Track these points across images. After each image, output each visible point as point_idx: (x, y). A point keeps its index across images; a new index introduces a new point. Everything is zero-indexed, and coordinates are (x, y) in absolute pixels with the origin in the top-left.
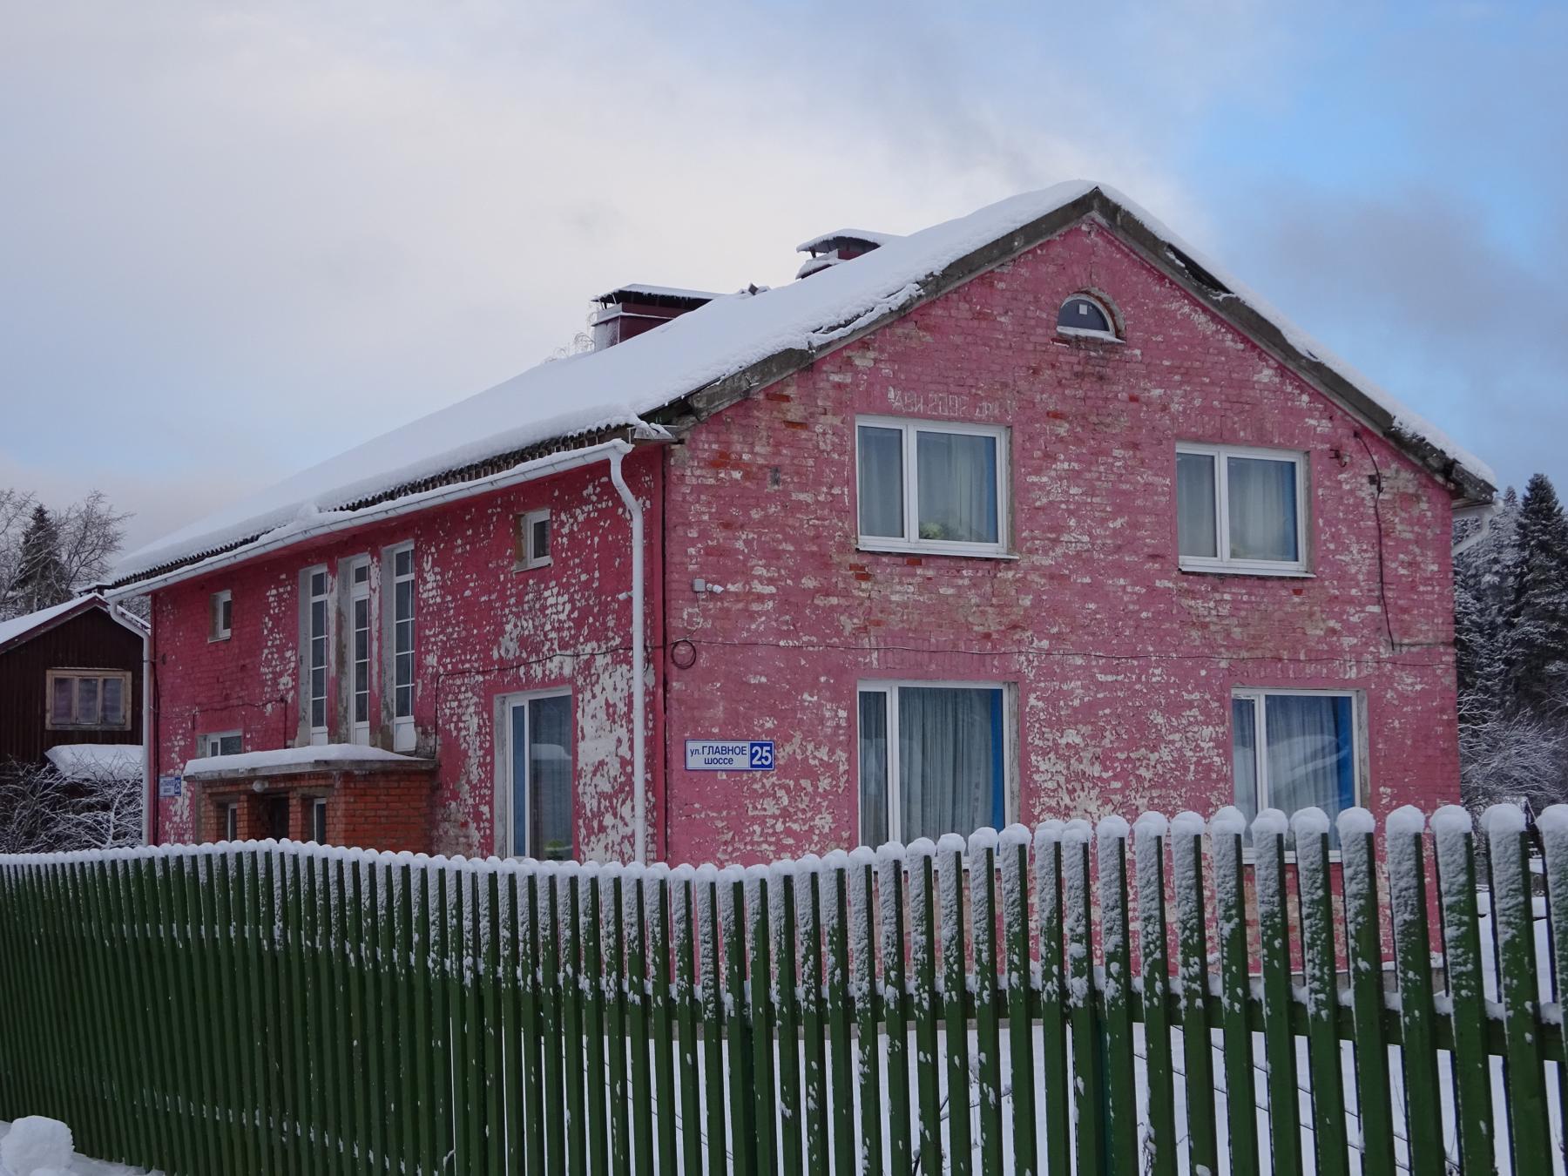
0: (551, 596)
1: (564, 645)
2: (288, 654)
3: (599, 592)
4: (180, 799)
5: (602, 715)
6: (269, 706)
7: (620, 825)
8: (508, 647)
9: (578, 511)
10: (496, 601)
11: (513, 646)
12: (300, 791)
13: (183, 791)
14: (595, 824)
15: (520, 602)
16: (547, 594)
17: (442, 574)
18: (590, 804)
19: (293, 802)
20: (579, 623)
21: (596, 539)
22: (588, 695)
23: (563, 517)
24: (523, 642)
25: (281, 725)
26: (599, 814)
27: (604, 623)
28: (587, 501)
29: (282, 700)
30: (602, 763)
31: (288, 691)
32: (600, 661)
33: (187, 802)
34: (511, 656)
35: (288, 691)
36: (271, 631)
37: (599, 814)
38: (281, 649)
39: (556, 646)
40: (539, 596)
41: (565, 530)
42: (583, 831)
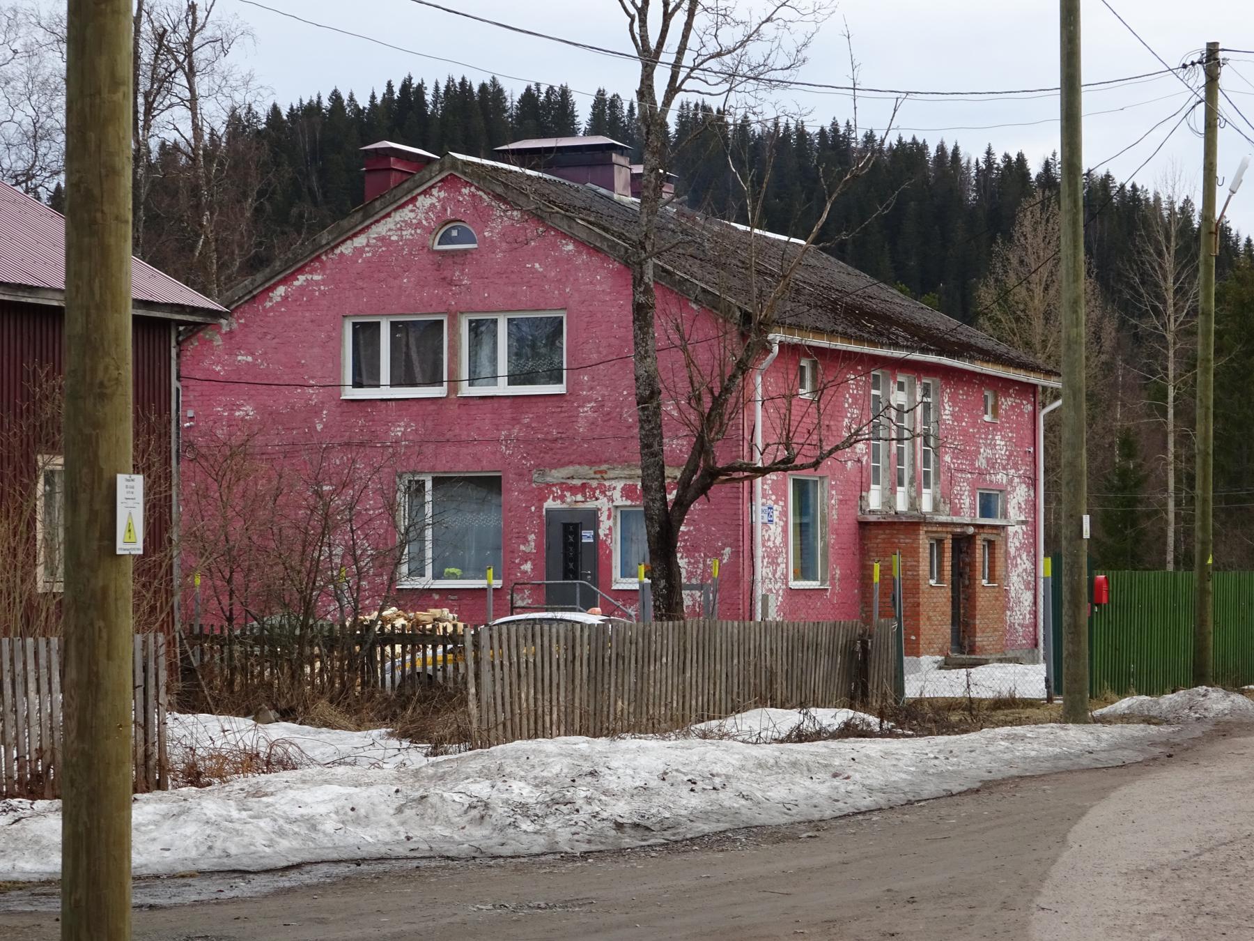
1: (1004, 468)
4: (772, 526)
6: (849, 463)
8: (981, 462)
11: (984, 461)
12: (984, 536)
13: (776, 519)
15: (986, 439)
17: (954, 406)
18: (1012, 551)
19: (978, 542)
24: (988, 460)
25: (858, 479)
26: (1015, 557)
29: (859, 461)
31: (863, 455)
32: (1016, 480)
35: (863, 455)
36: (850, 406)
37: (1015, 557)
40: (993, 439)
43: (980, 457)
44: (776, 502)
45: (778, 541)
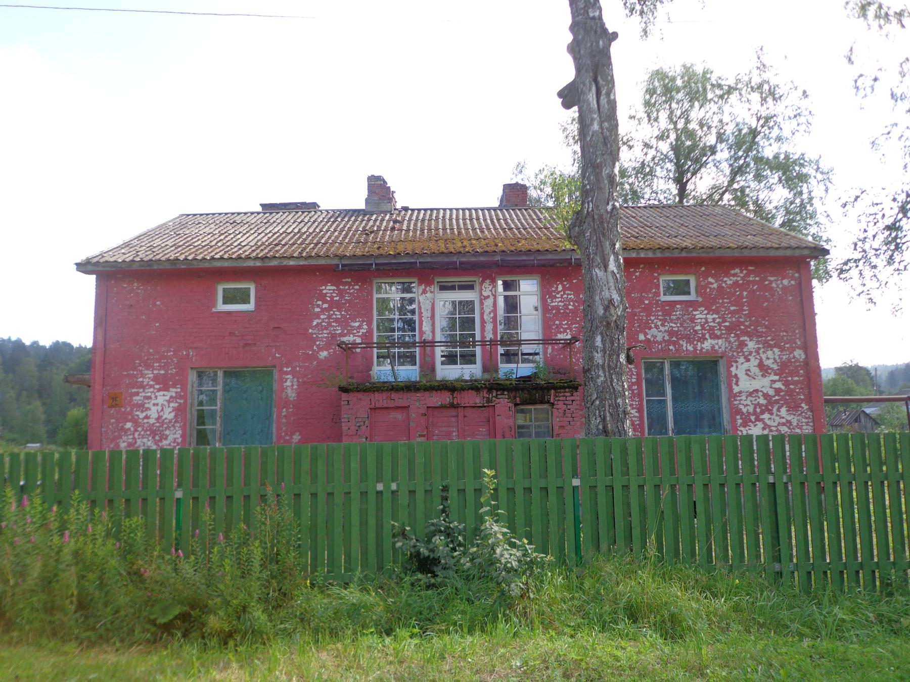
0: (700, 315)
1: (714, 337)
2: (357, 324)
3: (748, 316)
5: (755, 370)
7: (777, 419)
9: (725, 279)
10: (640, 312)
14: (753, 418)
16: (695, 313)
17: (577, 295)
20: (729, 329)
21: (745, 293)
22: (742, 360)
23: (710, 280)
24: (671, 333)
27: (755, 329)
28: (735, 275)
30: (757, 391)
33: (171, 409)
34: (659, 339)
38: (344, 322)
39: (707, 336)
41: (715, 286)
42: (739, 421)
43: (654, 331)
44: (166, 388)
45: (169, 415)
